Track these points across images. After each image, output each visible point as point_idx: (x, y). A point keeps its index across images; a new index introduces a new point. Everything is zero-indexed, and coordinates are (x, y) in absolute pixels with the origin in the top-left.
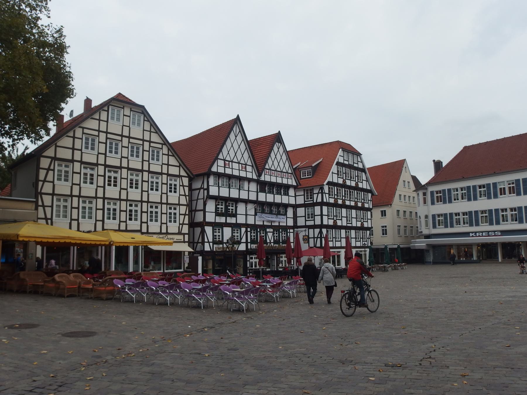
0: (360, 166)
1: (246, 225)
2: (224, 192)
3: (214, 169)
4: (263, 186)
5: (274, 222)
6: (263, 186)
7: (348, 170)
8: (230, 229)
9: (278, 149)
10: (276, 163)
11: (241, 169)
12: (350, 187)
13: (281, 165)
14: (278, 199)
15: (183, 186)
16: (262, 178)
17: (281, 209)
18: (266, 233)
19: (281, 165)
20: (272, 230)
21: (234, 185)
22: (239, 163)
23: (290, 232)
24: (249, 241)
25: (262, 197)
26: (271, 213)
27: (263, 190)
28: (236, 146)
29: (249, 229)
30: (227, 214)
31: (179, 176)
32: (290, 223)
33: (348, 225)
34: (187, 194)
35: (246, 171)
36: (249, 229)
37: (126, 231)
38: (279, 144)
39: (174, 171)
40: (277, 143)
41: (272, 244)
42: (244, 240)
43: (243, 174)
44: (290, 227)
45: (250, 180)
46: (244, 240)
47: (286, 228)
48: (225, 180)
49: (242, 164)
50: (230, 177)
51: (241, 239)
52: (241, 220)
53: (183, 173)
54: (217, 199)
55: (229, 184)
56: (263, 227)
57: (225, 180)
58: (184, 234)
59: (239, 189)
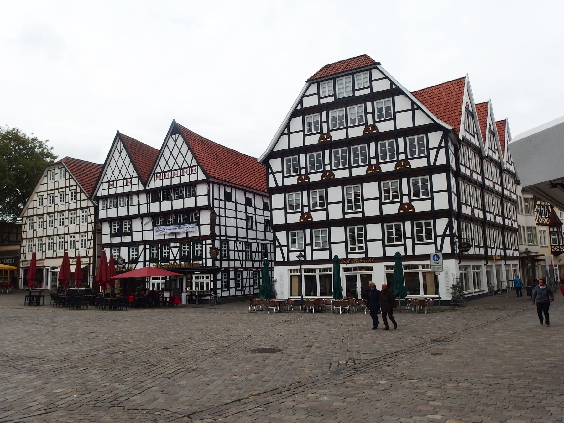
0: (384, 86)
1: (144, 243)
2: (112, 213)
3: (99, 194)
4: (155, 195)
5: (179, 233)
6: (155, 195)
7: (337, 113)
8: (127, 248)
9: (175, 142)
10: (171, 162)
11: (125, 184)
12: (349, 142)
13: (180, 160)
14: (178, 204)
15: (90, 215)
16: (151, 186)
17: (190, 215)
18: (170, 248)
19: (180, 160)
20: (178, 244)
21: (122, 203)
22: (124, 179)
23: (206, 244)
24: (147, 259)
25: (155, 208)
26: (175, 223)
27: (156, 199)
28: (120, 163)
29: (147, 247)
30: (120, 234)
31: (88, 207)
32: (206, 231)
33: (347, 216)
34: (93, 221)
35: (124, 186)
36: (147, 247)
37: (57, 257)
38: (177, 135)
39: (84, 204)
40: (173, 136)
41: (178, 262)
42: (141, 259)
43: (127, 189)
44: (206, 238)
45: (138, 193)
46: (141, 259)
47: (200, 240)
48: (113, 201)
49: (127, 179)
50: (117, 196)
51: (138, 258)
52: (137, 237)
53: (90, 204)
54: (110, 220)
55: (117, 204)
56: (166, 243)
57: (113, 201)
58: (90, 257)
59: (128, 206)
